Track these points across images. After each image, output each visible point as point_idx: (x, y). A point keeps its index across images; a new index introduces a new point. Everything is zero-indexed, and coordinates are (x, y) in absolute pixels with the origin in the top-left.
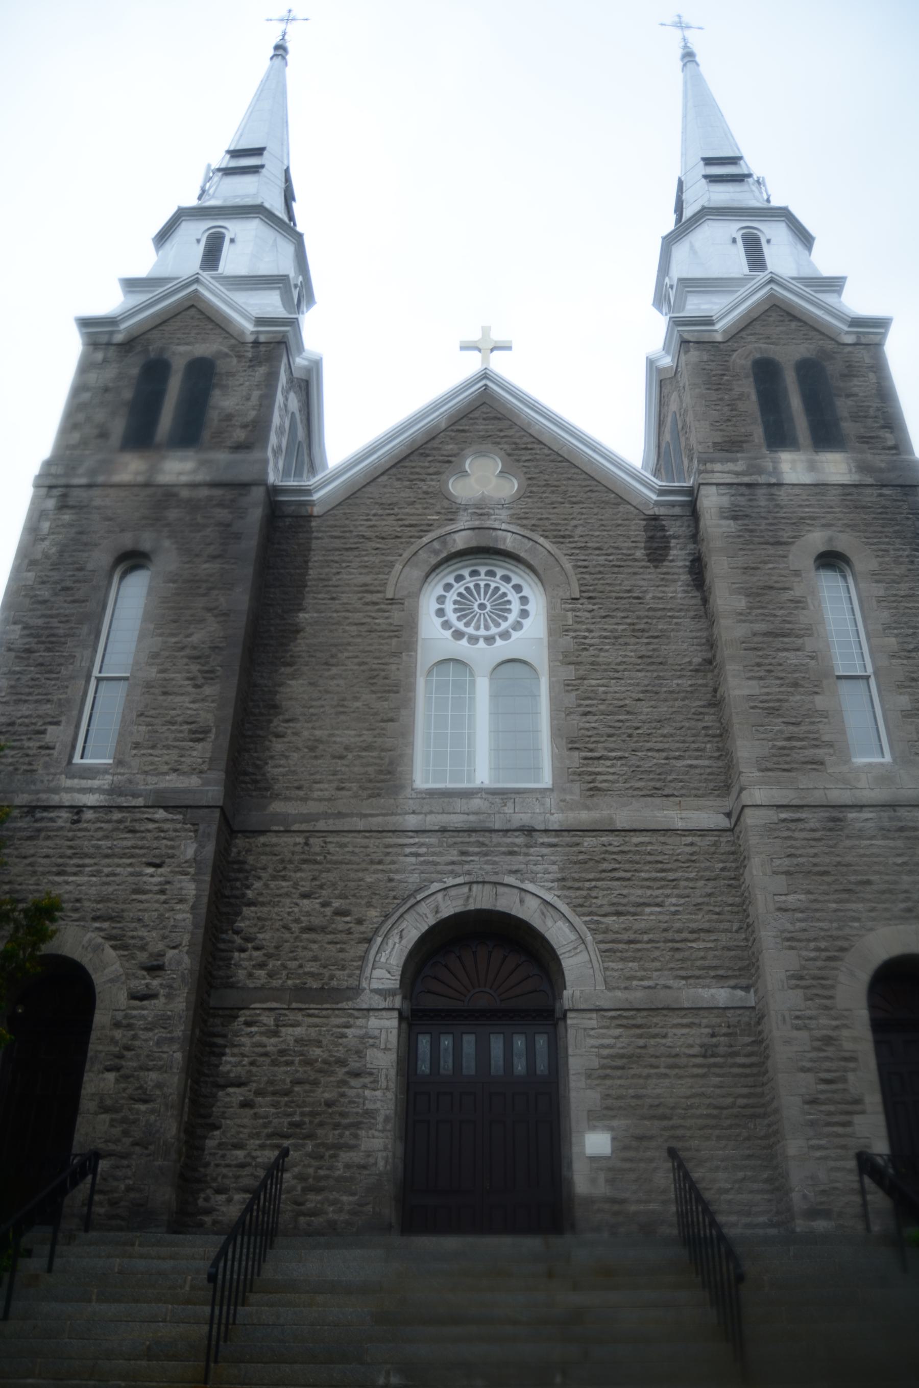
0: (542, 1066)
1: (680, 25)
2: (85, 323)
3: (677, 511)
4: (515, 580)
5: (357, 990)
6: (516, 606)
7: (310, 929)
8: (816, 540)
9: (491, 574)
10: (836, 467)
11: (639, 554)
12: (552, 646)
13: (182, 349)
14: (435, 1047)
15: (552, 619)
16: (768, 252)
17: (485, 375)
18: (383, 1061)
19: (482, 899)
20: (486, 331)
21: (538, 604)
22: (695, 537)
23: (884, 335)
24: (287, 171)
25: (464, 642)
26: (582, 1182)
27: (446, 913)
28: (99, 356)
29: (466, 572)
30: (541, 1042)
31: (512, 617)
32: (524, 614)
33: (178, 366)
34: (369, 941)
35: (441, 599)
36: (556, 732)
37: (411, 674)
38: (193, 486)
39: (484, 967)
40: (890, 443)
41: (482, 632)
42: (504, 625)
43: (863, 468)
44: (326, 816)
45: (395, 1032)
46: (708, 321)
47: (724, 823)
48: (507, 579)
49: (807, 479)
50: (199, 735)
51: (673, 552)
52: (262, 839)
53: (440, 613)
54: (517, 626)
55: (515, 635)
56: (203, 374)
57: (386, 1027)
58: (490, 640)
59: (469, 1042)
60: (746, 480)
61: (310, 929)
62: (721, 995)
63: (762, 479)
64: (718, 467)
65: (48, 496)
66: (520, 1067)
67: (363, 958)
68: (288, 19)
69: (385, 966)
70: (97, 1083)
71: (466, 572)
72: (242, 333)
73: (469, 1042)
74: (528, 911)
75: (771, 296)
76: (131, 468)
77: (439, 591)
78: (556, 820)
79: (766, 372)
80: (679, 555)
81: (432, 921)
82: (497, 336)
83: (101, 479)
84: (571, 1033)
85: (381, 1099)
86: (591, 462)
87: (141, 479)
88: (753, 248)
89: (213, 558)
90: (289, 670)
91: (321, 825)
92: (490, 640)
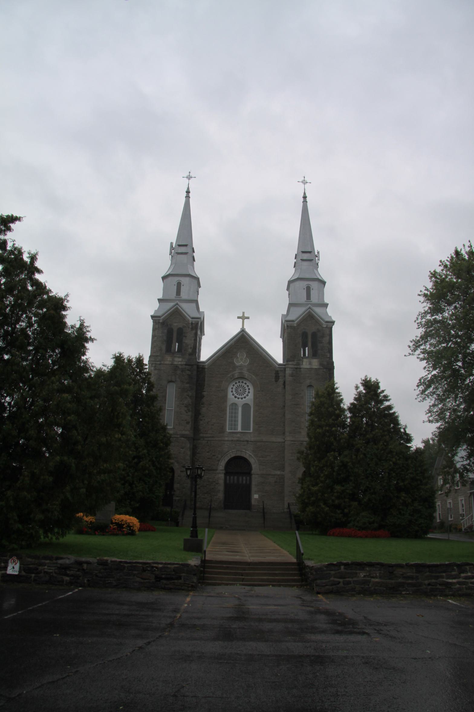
0: (248, 482)
1: (304, 182)
2: (152, 317)
3: (282, 369)
4: (248, 384)
5: (217, 470)
6: (247, 391)
7: (209, 458)
8: (308, 382)
9: (242, 382)
10: (315, 363)
11: (274, 380)
12: (254, 402)
13: (175, 324)
14: (230, 478)
15: (255, 395)
16: (312, 292)
17: (243, 330)
18: (222, 482)
19: (239, 454)
20: (243, 313)
21: (252, 391)
22: (285, 376)
23: (333, 325)
24: (193, 249)
25: (236, 399)
26: (253, 502)
27: (233, 455)
28: (157, 326)
29: (237, 382)
30: (248, 478)
31: (247, 393)
32: (249, 392)
33: (175, 330)
34: (219, 461)
35: (232, 388)
36: (254, 421)
37: (226, 407)
38: (181, 365)
39: (239, 466)
40: (328, 356)
41: (240, 397)
42: (245, 395)
43: (321, 364)
44: (210, 437)
45: (223, 477)
46: (293, 321)
47: (283, 440)
48: (246, 384)
49: (308, 367)
50: (188, 423)
51: (280, 380)
52: (199, 441)
53: (232, 391)
54: (247, 395)
55: (247, 397)
56: (181, 332)
57: (222, 476)
58: (242, 398)
59: (236, 477)
60: (296, 367)
61: (209, 458)
62: (278, 472)
63: (298, 367)
64: (290, 363)
65: (152, 366)
66: (244, 482)
67: (218, 464)
68: (189, 177)
69: (222, 466)
70: (176, 486)
71: (237, 382)
72: (189, 320)
73: (236, 477)
74: (246, 456)
75: (309, 312)
76: (168, 359)
77: (232, 386)
78: (253, 439)
79: (305, 335)
80: (281, 380)
81: (230, 457)
82: (246, 315)
83: (162, 362)
84: (253, 479)
85: (221, 488)
86: (265, 356)
87: (170, 363)
88: (308, 289)
89: (187, 383)
90: (202, 406)
91: (210, 439)
92: (242, 398)
